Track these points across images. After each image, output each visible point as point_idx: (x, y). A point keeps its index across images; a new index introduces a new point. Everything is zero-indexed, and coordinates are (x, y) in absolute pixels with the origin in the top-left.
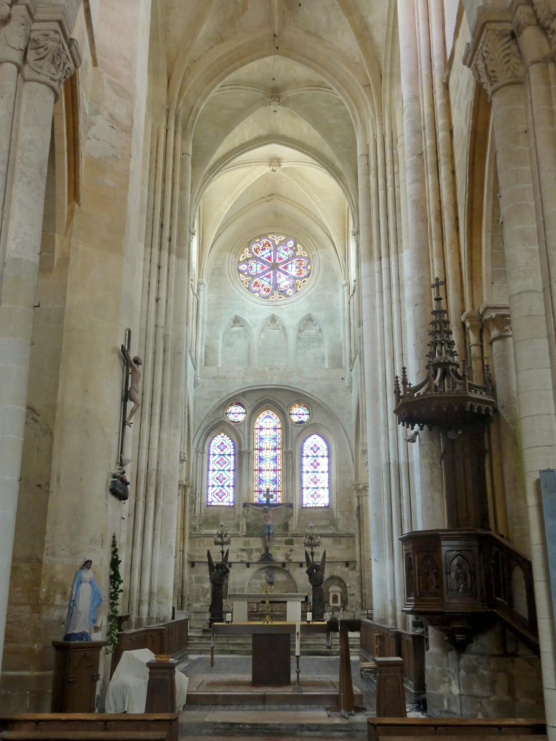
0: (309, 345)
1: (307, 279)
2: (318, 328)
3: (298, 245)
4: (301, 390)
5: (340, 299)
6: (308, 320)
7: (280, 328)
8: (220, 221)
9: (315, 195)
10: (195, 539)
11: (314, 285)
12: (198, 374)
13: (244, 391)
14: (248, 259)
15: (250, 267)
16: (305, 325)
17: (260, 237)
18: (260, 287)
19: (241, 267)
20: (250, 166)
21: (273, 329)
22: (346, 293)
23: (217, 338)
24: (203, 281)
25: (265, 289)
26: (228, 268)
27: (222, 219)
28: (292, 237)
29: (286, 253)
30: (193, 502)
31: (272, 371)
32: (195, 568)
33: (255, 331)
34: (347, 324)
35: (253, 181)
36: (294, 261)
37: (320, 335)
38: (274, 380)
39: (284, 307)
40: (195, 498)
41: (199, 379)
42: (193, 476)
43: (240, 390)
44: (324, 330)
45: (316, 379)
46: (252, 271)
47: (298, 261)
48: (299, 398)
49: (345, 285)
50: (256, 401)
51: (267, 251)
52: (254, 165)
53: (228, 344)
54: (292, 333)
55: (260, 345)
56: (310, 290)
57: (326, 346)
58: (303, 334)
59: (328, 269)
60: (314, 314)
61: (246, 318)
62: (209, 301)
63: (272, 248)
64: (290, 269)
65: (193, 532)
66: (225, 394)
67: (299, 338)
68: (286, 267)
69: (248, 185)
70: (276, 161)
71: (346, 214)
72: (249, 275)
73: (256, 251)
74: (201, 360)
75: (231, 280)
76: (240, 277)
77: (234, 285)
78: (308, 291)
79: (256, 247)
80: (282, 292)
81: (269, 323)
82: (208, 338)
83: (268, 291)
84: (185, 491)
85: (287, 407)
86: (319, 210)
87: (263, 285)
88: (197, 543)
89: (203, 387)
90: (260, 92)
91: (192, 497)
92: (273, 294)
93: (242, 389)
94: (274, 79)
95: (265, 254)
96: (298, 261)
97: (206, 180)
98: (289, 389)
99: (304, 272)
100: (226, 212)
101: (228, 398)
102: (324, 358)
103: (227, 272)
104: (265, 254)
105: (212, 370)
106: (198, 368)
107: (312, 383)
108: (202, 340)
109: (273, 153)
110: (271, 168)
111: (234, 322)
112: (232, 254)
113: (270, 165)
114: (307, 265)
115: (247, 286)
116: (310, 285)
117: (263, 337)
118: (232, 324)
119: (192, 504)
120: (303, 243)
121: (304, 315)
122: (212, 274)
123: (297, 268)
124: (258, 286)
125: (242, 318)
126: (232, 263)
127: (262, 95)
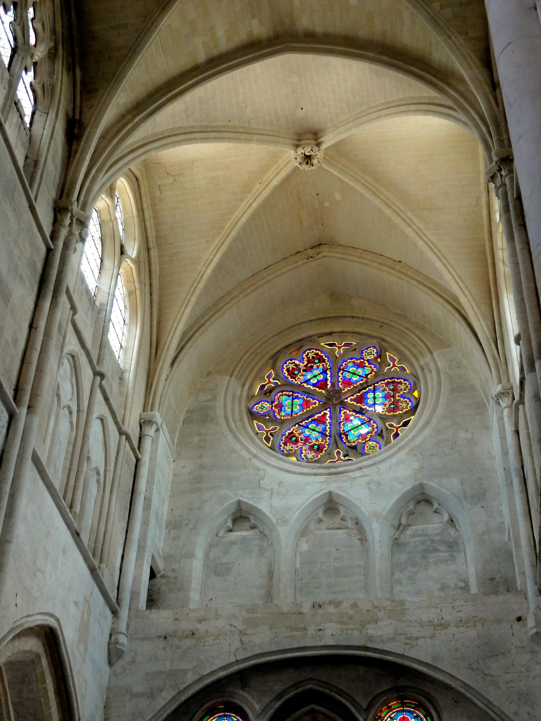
0: (424, 557)
1: (412, 417)
2: (446, 517)
3: (387, 354)
4: (403, 656)
5: (495, 439)
6: (419, 502)
7: (350, 524)
8: (198, 291)
9: (409, 214)
11: (428, 423)
12: (123, 627)
13: (242, 666)
14: (271, 391)
15: (276, 407)
16: (411, 513)
17: (299, 345)
18: (300, 444)
19: (257, 408)
20: (249, 141)
21: (332, 529)
22: (506, 412)
23: (191, 555)
24: (154, 416)
25: (311, 448)
26: (225, 406)
27: (201, 286)
28: (371, 337)
29: (360, 371)
31: (321, 611)
33: (285, 535)
34: (516, 482)
35: (265, 194)
36: (381, 385)
37: (452, 532)
38: (327, 634)
39: (357, 474)
41: (123, 639)
43: (230, 665)
44: (462, 520)
45: (444, 626)
46: (283, 413)
47: (388, 384)
48: (402, 683)
49: (501, 395)
50: (278, 697)
51: (316, 372)
52: (259, 141)
53: (216, 569)
54: (378, 533)
55: (298, 565)
56: (419, 433)
57: (469, 555)
58: (409, 532)
59: (460, 388)
60: (434, 486)
61: (263, 506)
62: (175, 475)
63: (328, 365)
64: (371, 401)
66: (190, 678)
67: (396, 544)
68: (361, 399)
69: (255, 205)
70: (308, 135)
71: (487, 244)
72: (274, 420)
73: (292, 373)
74: (135, 594)
75: (231, 430)
76: (252, 427)
77: (235, 437)
78: (414, 437)
79: (291, 366)
80: (355, 448)
81: (320, 514)
82: (167, 558)
83: (320, 449)
85: (367, 710)
86: (420, 243)
87: (307, 439)
89: (134, 662)
92: (330, 454)
93: (237, 662)
95: (315, 375)
96: (388, 384)
98: (369, 654)
99: (405, 405)
100: (209, 271)
101: (197, 687)
102: (466, 588)
103: (220, 412)
104: (315, 375)
105: (162, 618)
106: (124, 613)
107: (432, 637)
108: (141, 549)
109: (300, 114)
110: (300, 151)
111: (234, 521)
112: (233, 378)
113: (297, 146)
114: (412, 391)
115: (269, 445)
116: (420, 424)
117: (304, 547)
118: (229, 524)
120: (401, 347)
121: (408, 487)
122: (187, 421)
123: (386, 397)
124: (297, 441)
125: (252, 507)
126: (234, 396)
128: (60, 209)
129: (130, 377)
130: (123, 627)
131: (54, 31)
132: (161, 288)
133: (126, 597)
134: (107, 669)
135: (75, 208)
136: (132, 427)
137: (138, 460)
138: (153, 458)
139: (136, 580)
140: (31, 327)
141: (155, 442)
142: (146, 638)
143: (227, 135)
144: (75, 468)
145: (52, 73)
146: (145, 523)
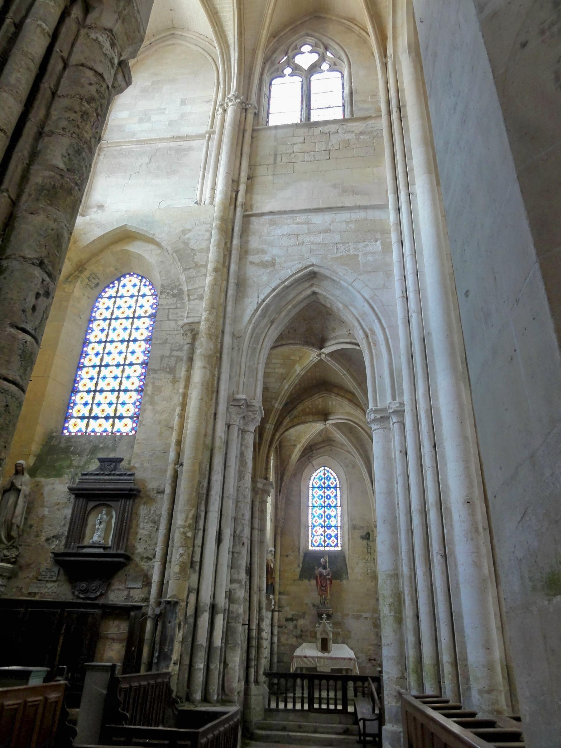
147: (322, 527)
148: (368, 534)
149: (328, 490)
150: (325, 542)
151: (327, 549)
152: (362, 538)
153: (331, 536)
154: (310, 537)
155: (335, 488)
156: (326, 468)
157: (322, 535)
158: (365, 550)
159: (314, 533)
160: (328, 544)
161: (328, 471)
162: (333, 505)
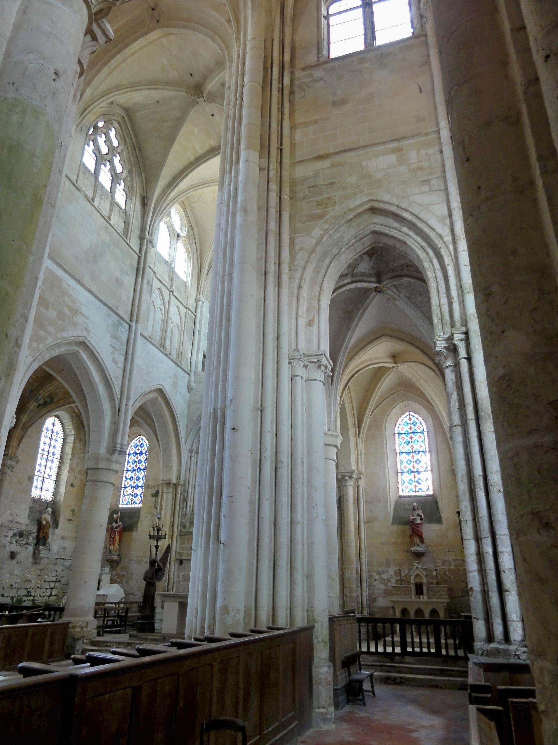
10: (184, 536)
12: (192, 380)
30: (185, 500)
32: (182, 566)
40: (187, 496)
41: (193, 384)
42: (186, 475)
65: (183, 530)
84: (176, 490)
88: (186, 541)
90: (182, 91)
91: (184, 496)
94: (191, 75)
97: (164, 195)
106: (193, 375)
119: (183, 502)
127: (184, 94)
128: (142, 238)
129: (189, 284)
130: (192, 380)
131: (129, 161)
132: (200, 244)
133: (193, 369)
134: (188, 394)
135: (147, 236)
136: (191, 304)
137: (195, 316)
138: (201, 314)
139: (197, 362)
140: (134, 290)
141: (202, 308)
142: (200, 383)
143: (211, 184)
144: (165, 330)
145: (131, 180)
146: (199, 340)
147: (132, 487)
148: (158, 492)
149: (140, 456)
150: (132, 500)
151: (133, 506)
152: (153, 495)
153: (137, 495)
154: (121, 497)
155: (130, 454)
156: (141, 437)
157: (130, 494)
158: (153, 506)
159: (125, 493)
160: (134, 502)
161: (142, 439)
162: (142, 468)
